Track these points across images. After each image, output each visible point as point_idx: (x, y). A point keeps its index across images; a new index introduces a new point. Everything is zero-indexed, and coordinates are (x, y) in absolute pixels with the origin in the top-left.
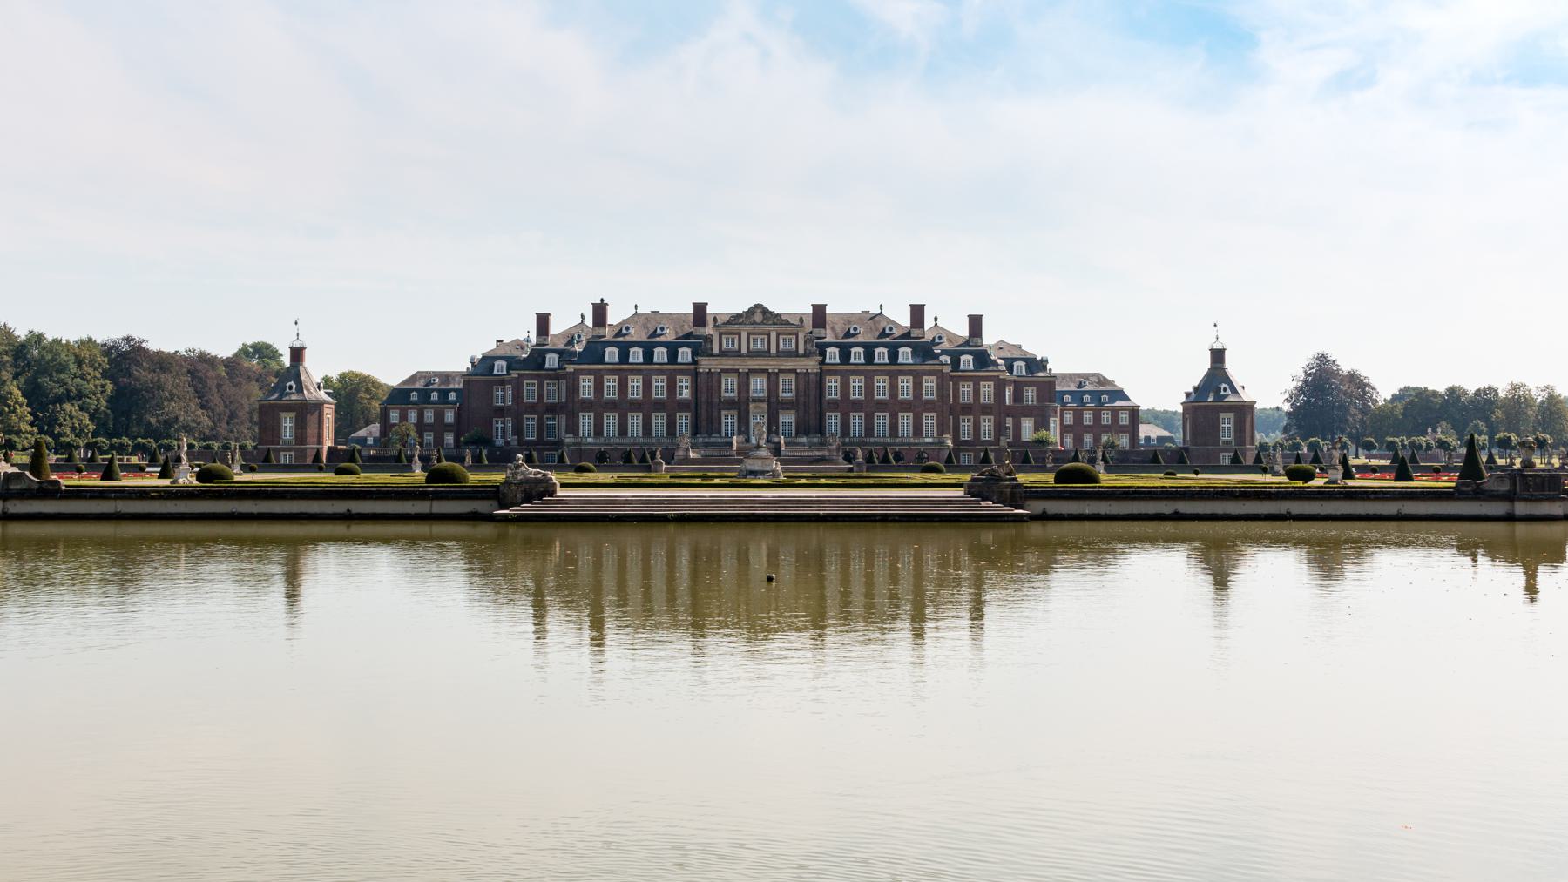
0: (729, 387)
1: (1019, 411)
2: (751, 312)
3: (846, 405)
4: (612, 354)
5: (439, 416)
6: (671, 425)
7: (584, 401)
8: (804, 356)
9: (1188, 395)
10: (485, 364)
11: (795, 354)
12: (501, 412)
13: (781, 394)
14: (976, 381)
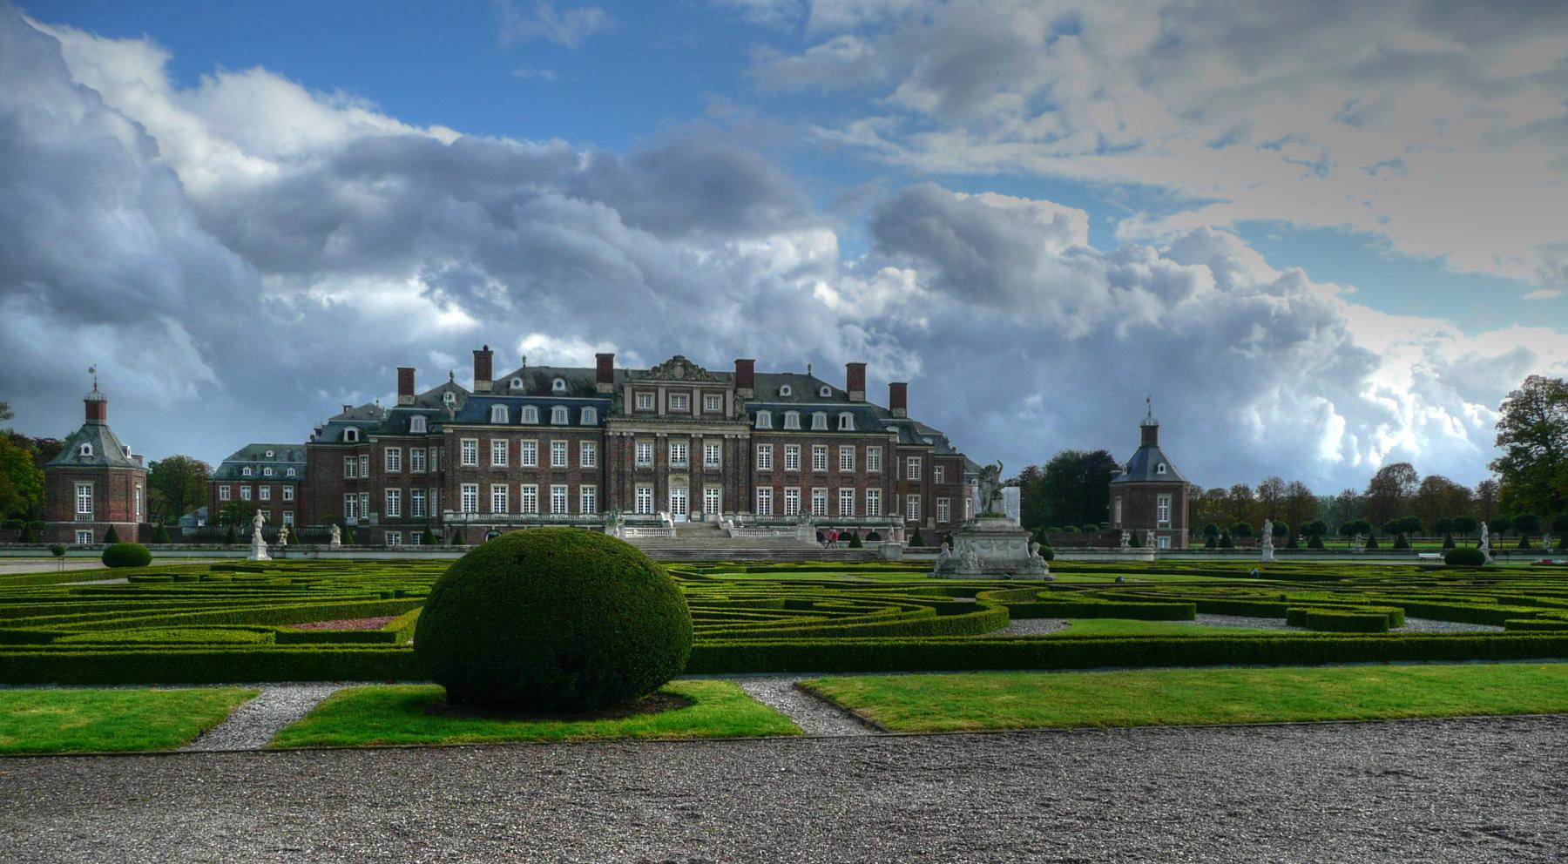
4: (500, 413)
6: (574, 498)
11: (721, 418)
12: (355, 486)
13: (705, 464)
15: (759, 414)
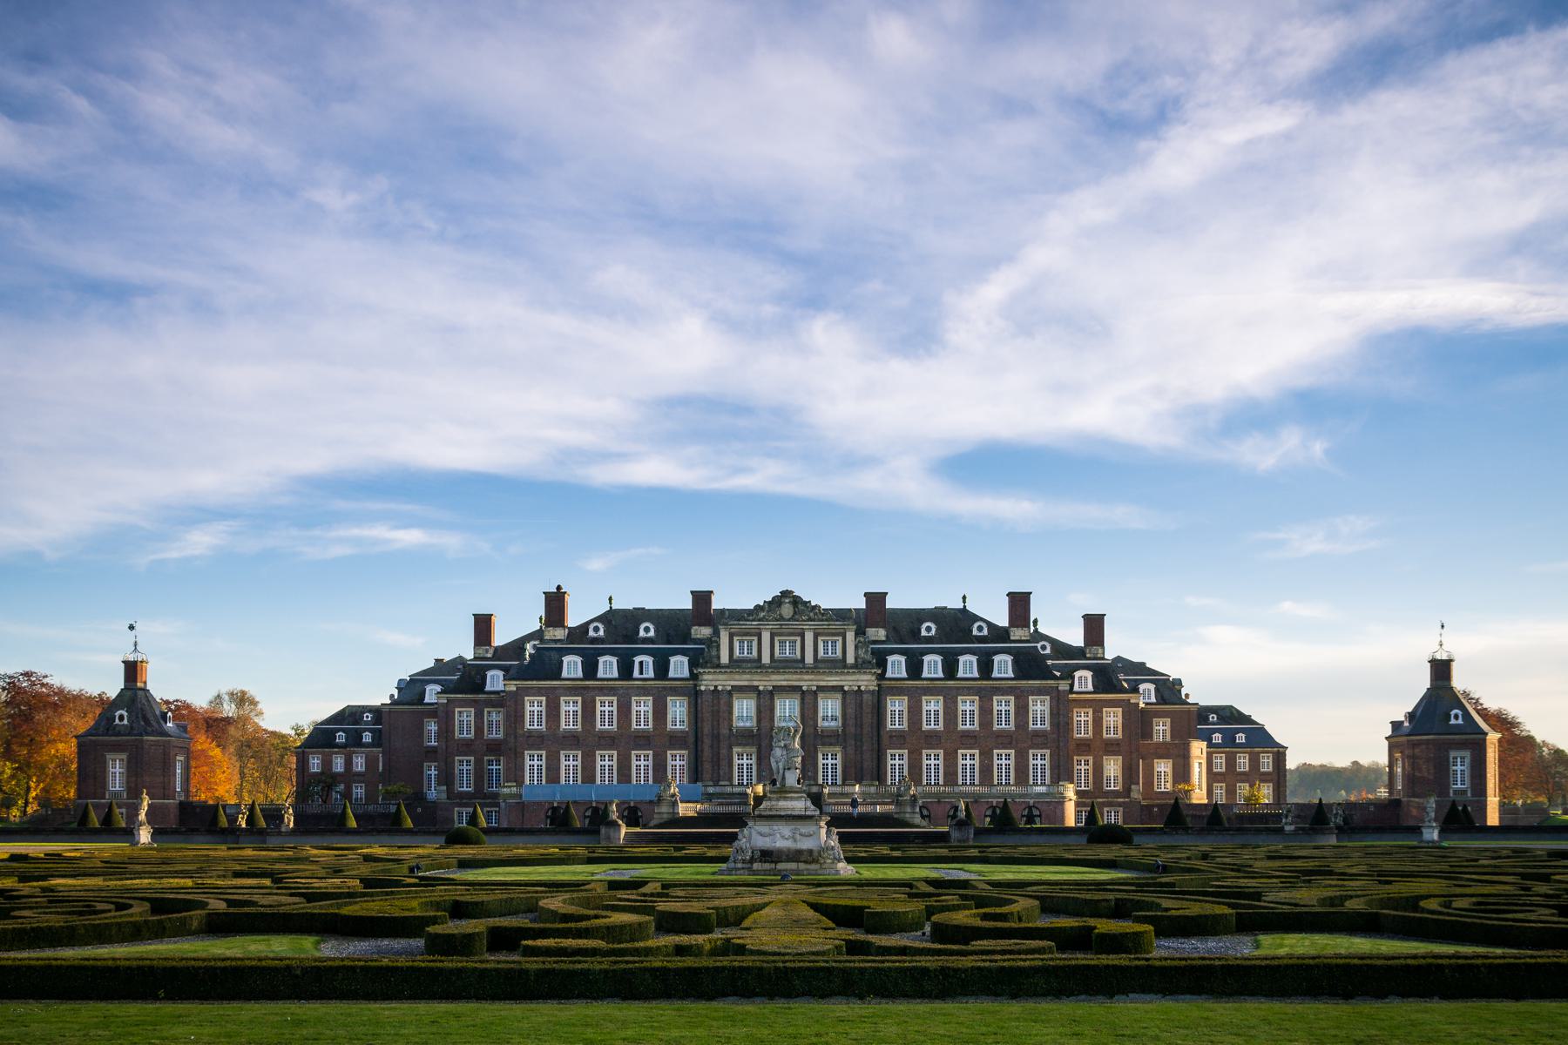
2: (776, 602)
3: (915, 739)
4: (572, 666)
6: (660, 768)
7: (530, 733)
9: (1396, 725)
10: (411, 688)
11: (839, 665)
12: (431, 753)
13: (820, 723)
14: (1098, 707)
15: (890, 659)
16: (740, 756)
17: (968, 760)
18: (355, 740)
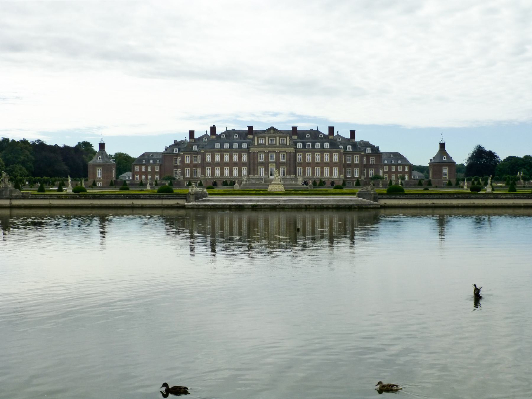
0: (261, 158)
1: (368, 166)
2: (269, 129)
5: (153, 169)
6: (240, 171)
8: (289, 146)
9: (431, 160)
12: (176, 167)
13: (281, 160)
16: (260, 168)
17: (318, 170)
18: (148, 161)
